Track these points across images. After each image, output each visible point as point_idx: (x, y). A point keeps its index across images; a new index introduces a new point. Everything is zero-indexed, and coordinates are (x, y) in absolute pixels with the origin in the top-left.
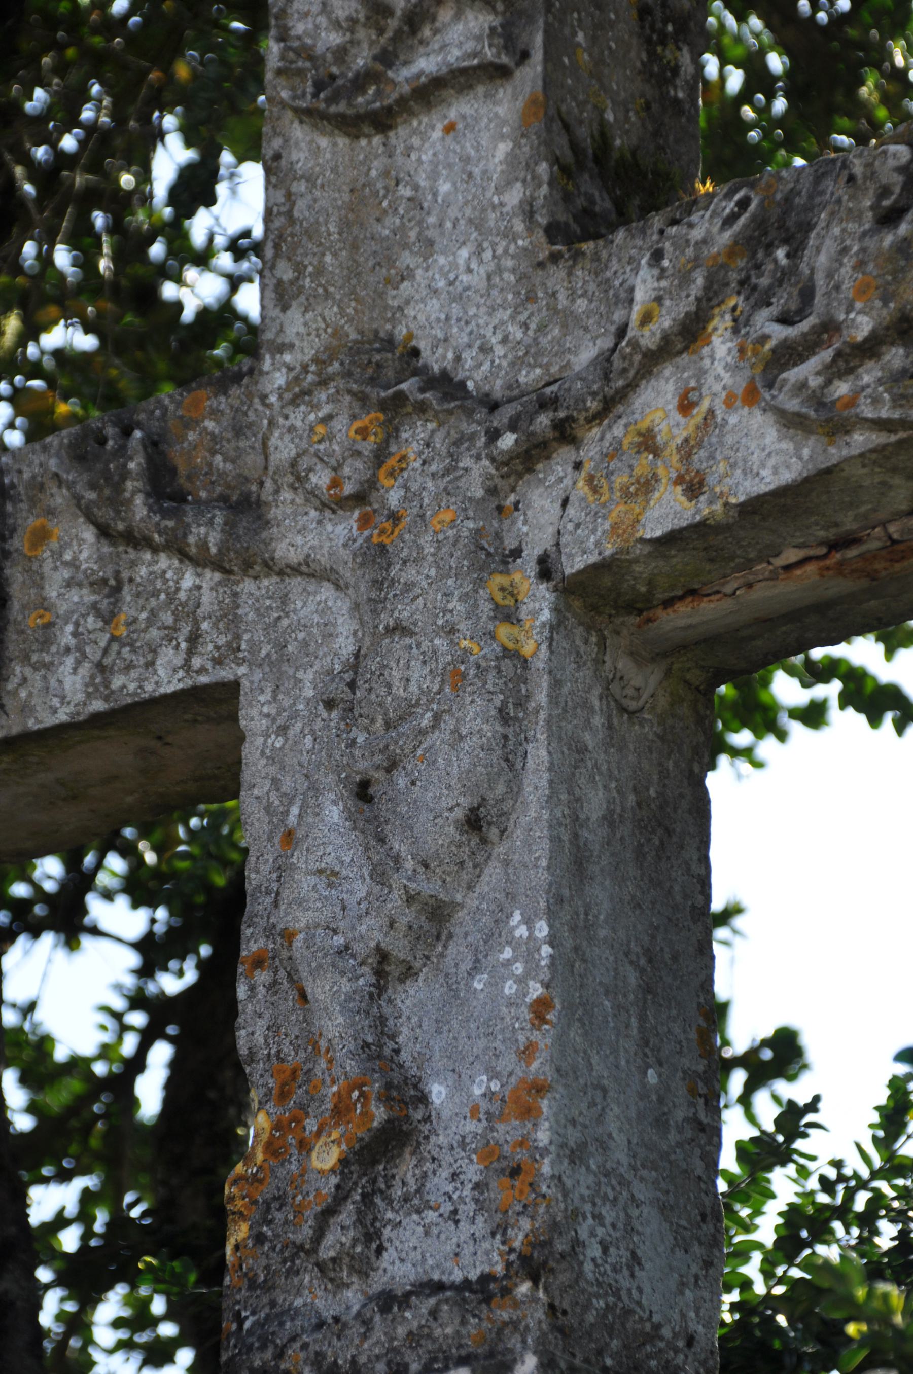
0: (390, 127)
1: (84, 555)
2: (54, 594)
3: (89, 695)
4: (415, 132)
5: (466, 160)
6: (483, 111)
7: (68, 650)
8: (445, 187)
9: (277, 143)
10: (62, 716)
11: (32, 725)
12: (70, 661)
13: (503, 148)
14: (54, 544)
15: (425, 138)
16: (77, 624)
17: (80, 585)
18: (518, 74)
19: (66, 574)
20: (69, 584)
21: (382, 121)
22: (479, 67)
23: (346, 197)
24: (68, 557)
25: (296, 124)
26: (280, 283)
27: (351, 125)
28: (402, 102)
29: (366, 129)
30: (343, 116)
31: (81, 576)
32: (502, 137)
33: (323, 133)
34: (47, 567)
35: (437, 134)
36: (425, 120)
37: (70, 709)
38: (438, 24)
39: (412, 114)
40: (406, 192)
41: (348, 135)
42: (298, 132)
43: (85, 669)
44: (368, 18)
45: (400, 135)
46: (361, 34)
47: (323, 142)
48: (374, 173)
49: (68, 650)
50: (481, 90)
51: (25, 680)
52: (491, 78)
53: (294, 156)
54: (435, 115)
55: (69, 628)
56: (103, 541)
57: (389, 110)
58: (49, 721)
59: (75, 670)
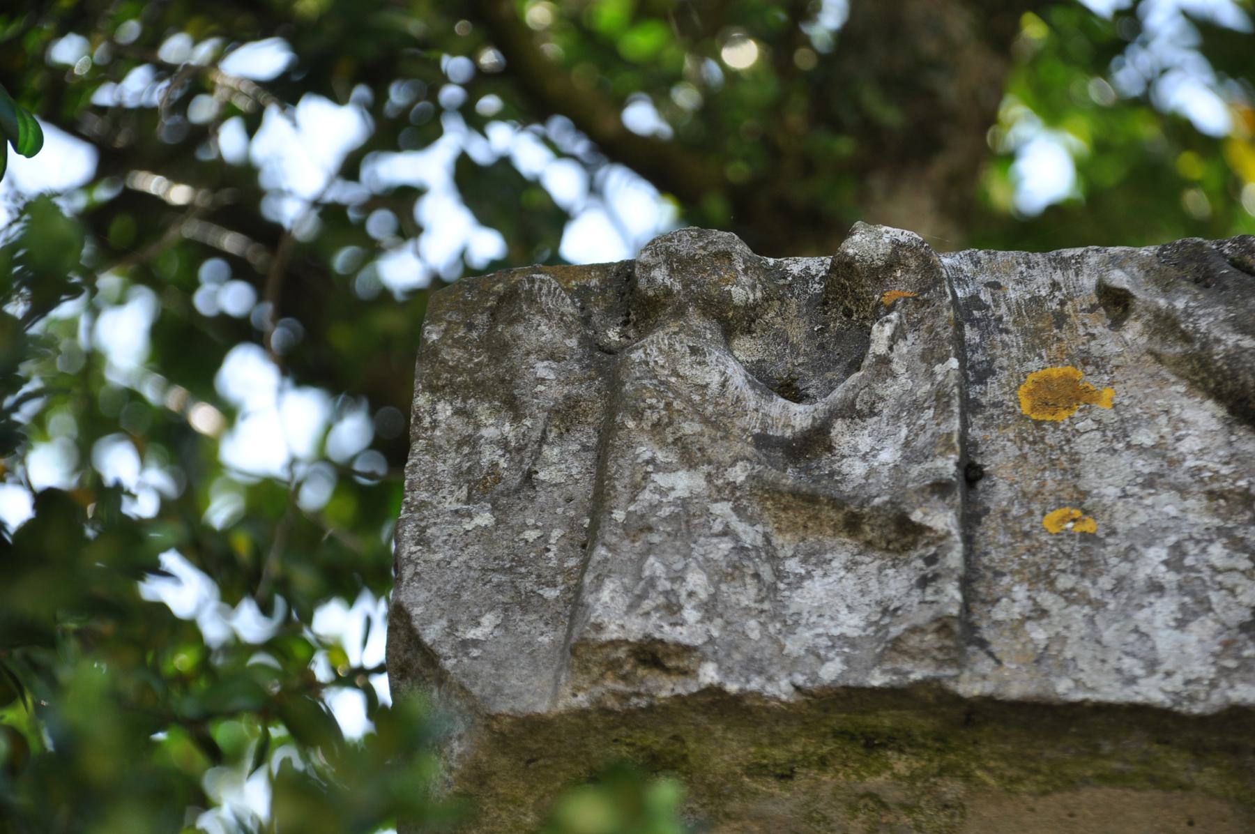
1: (1190, 444)
2: (1112, 492)
3: (1224, 672)
7: (1156, 588)
10: (1152, 691)
11: (1063, 688)
12: (1164, 609)
14: (1102, 408)
16: (1177, 548)
17: (1182, 491)
19: (1144, 466)
20: (1150, 482)
24: (1144, 437)
31: (1181, 476)
34: (1088, 445)
37: (1177, 682)
43: (1202, 631)
49: (1156, 588)
51: (1041, 613)
55: (1157, 554)
56: (1241, 432)
58: (1113, 692)
59: (1181, 624)
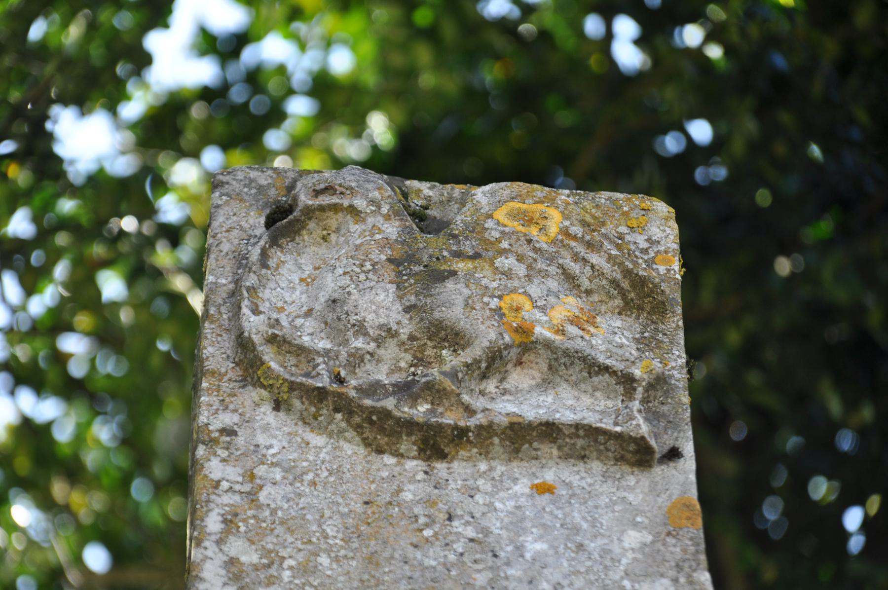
0: (442, 456)
4: (482, 475)
5: (577, 530)
6: (607, 487)
8: (534, 546)
9: (227, 419)
13: (633, 538)
15: (498, 484)
18: (659, 471)
21: (435, 444)
22: (618, 436)
23: (359, 508)
25: (267, 408)
26: (232, 562)
27: (380, 430)
28: (487, 431)
29: (407, 445)
30: (386, 414)
32: (635, 525)
33: (322, 430)
35: (522, 487)
36: (500, 468)
38: (506, 385)
39: (486, 454)
40: (470, 532)
41: (366, 443)
42: (267, 415)
44: (412, 338)
45: (457, 471)
46: (390, 351)
47: (318, 440)
48: (407, 496)
50: (596, 466)
52: (620, 459)
53: (261, 439)
54: (517, 468)
57: (460, 435)
